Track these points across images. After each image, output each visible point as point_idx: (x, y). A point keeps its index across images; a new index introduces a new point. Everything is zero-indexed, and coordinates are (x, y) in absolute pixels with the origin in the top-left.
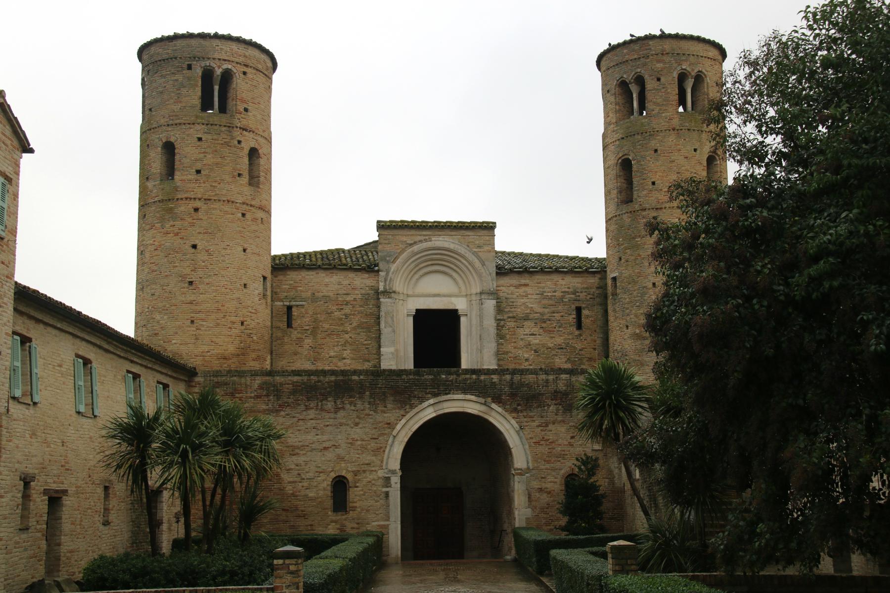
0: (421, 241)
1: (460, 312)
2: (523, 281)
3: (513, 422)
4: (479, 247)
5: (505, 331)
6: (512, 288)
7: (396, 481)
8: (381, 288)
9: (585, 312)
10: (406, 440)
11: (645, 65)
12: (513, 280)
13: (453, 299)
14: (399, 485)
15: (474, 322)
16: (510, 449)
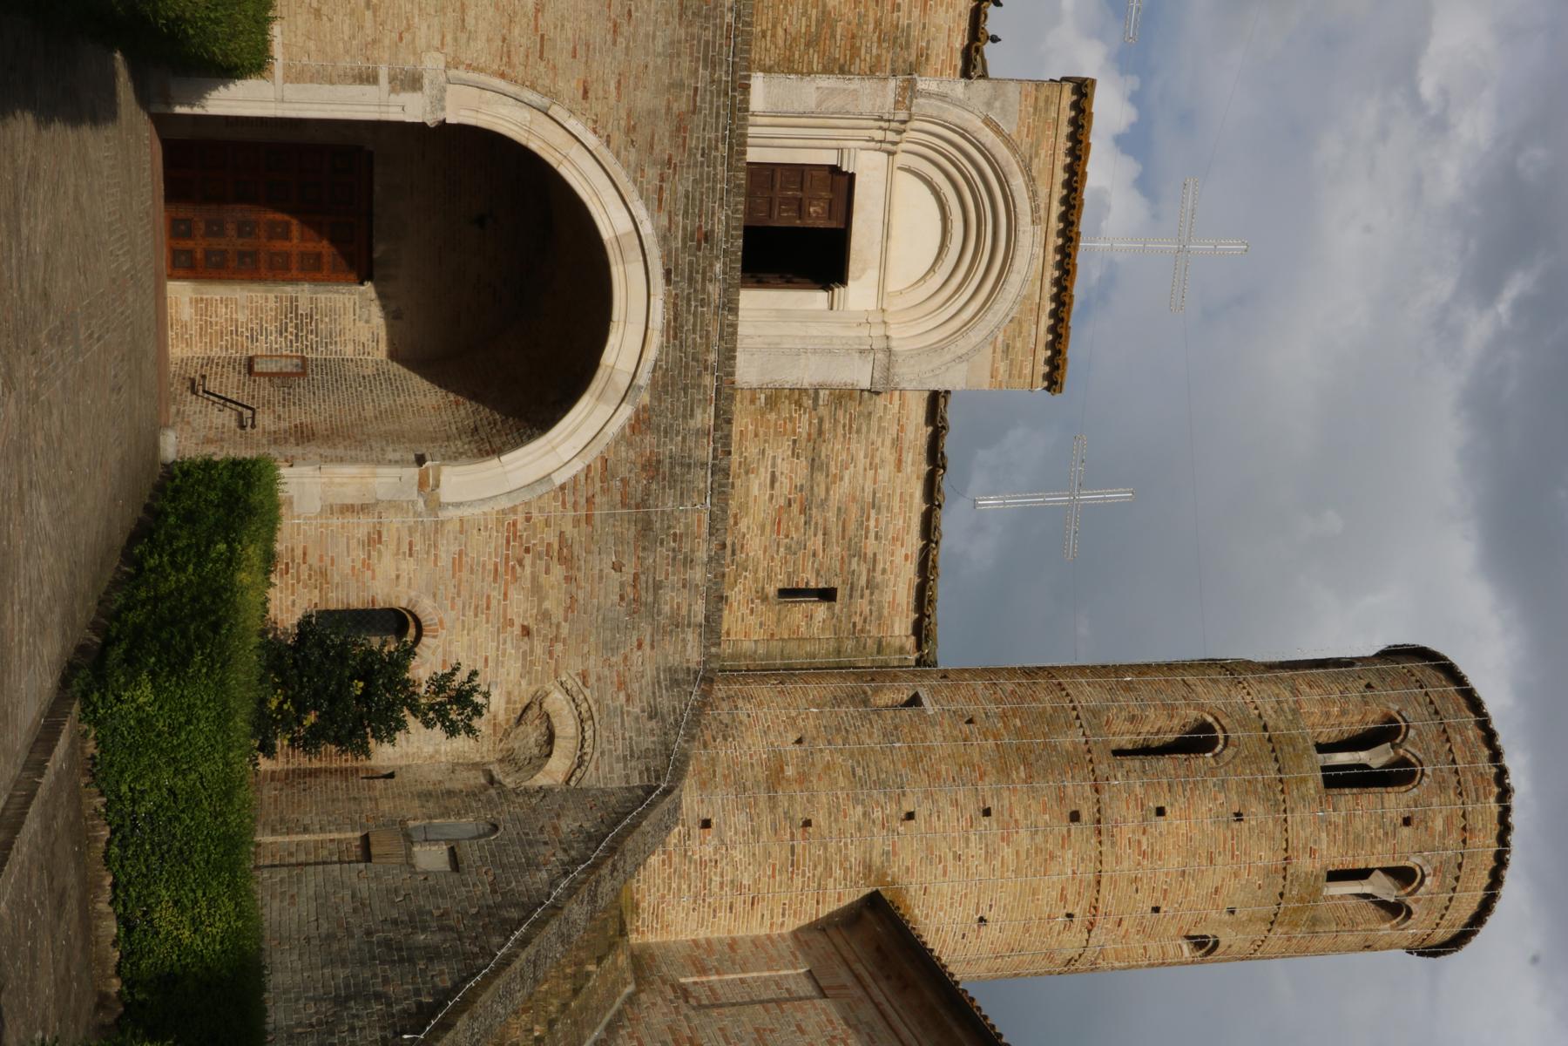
0: (1034, 195)
1: (839, 291)
2: (909, 458)
3: (578, 466)
4: (1007, 349)
5: (786, 408)
6: (894, 430)
7: (411, 109)
8: (922, 84)
9: (821, 610)
10: (534, 145)
11: (1442, 786)
12: (917, 432)
13: (873, 274)
14: (394, 115)
15: (815, 330)
16: (497, 452)
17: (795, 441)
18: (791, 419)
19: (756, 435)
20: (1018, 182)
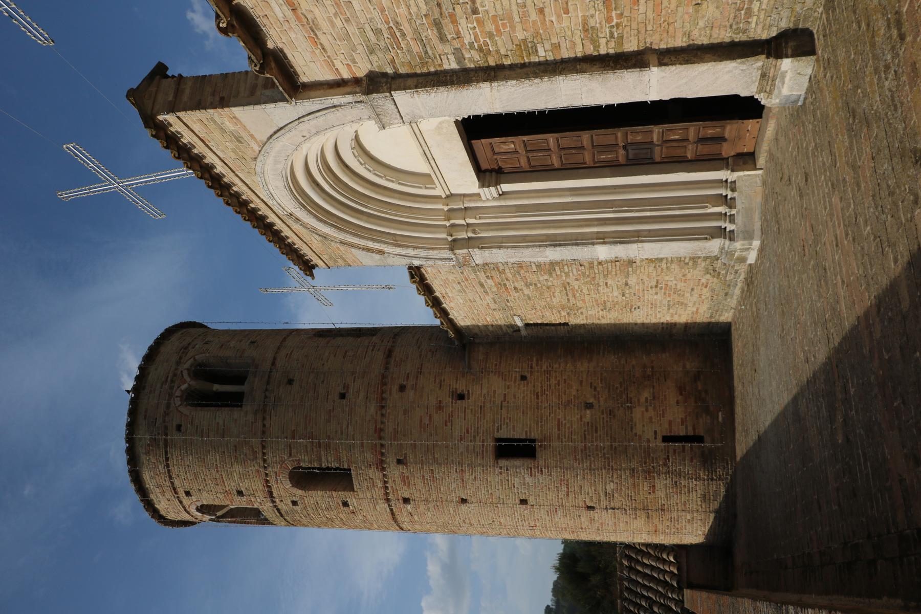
17: (475, 11)
18: (491, 35)
19: (541, 11)
20: (326, 230)
